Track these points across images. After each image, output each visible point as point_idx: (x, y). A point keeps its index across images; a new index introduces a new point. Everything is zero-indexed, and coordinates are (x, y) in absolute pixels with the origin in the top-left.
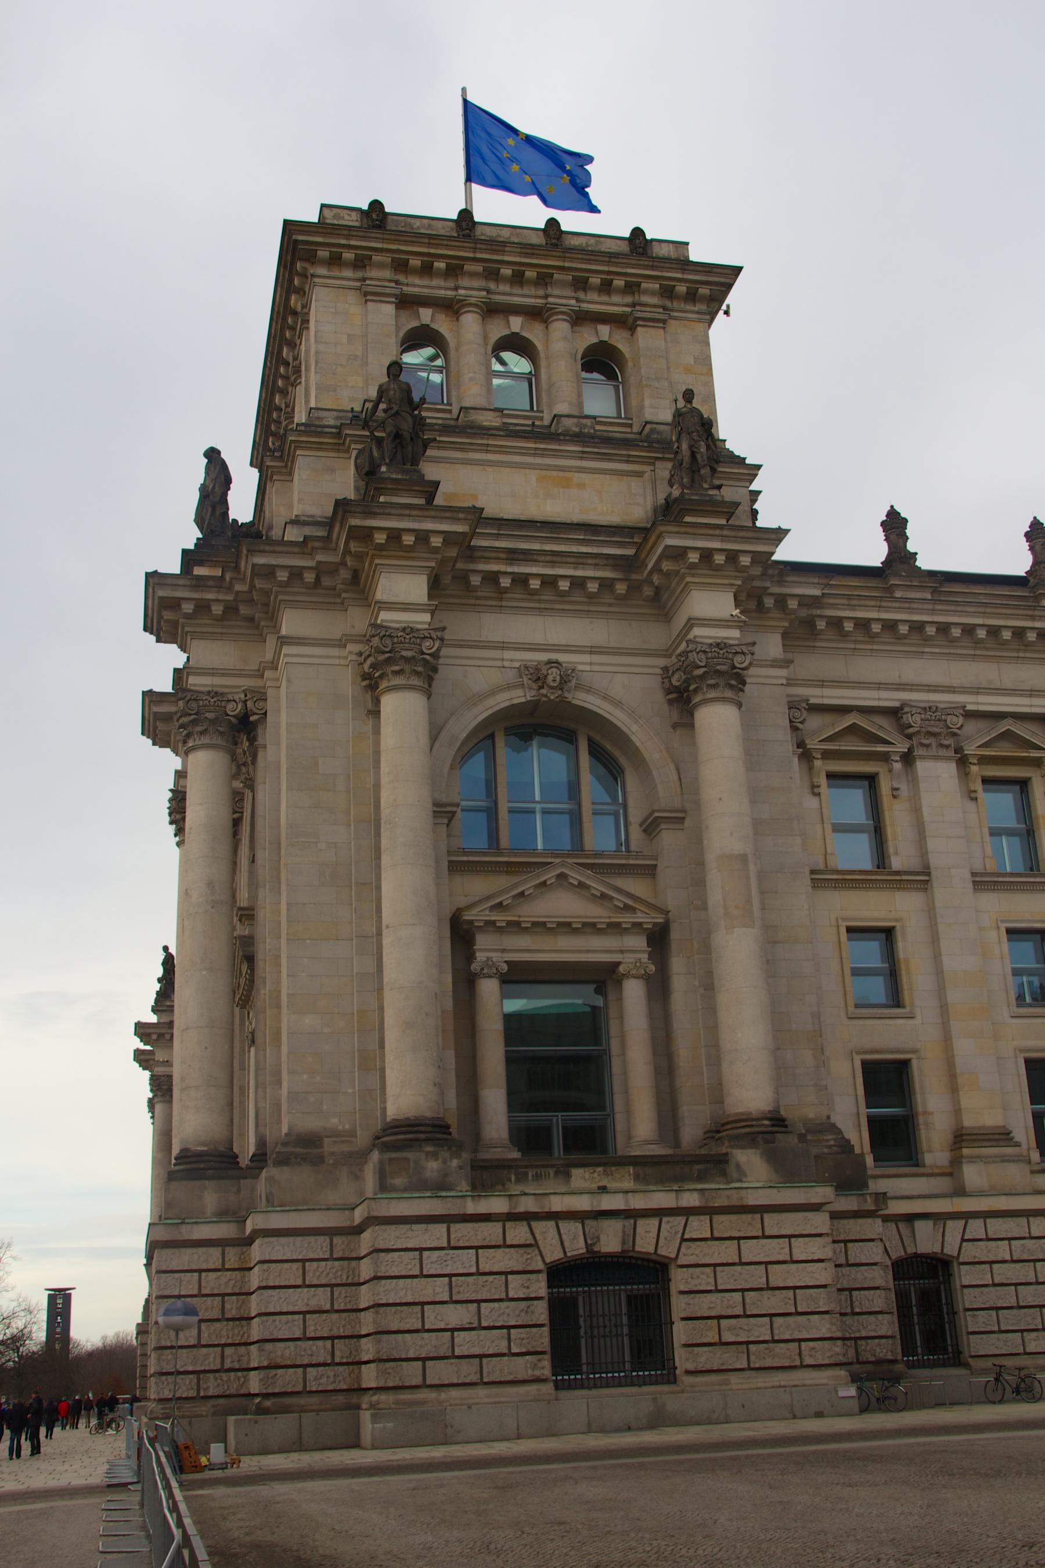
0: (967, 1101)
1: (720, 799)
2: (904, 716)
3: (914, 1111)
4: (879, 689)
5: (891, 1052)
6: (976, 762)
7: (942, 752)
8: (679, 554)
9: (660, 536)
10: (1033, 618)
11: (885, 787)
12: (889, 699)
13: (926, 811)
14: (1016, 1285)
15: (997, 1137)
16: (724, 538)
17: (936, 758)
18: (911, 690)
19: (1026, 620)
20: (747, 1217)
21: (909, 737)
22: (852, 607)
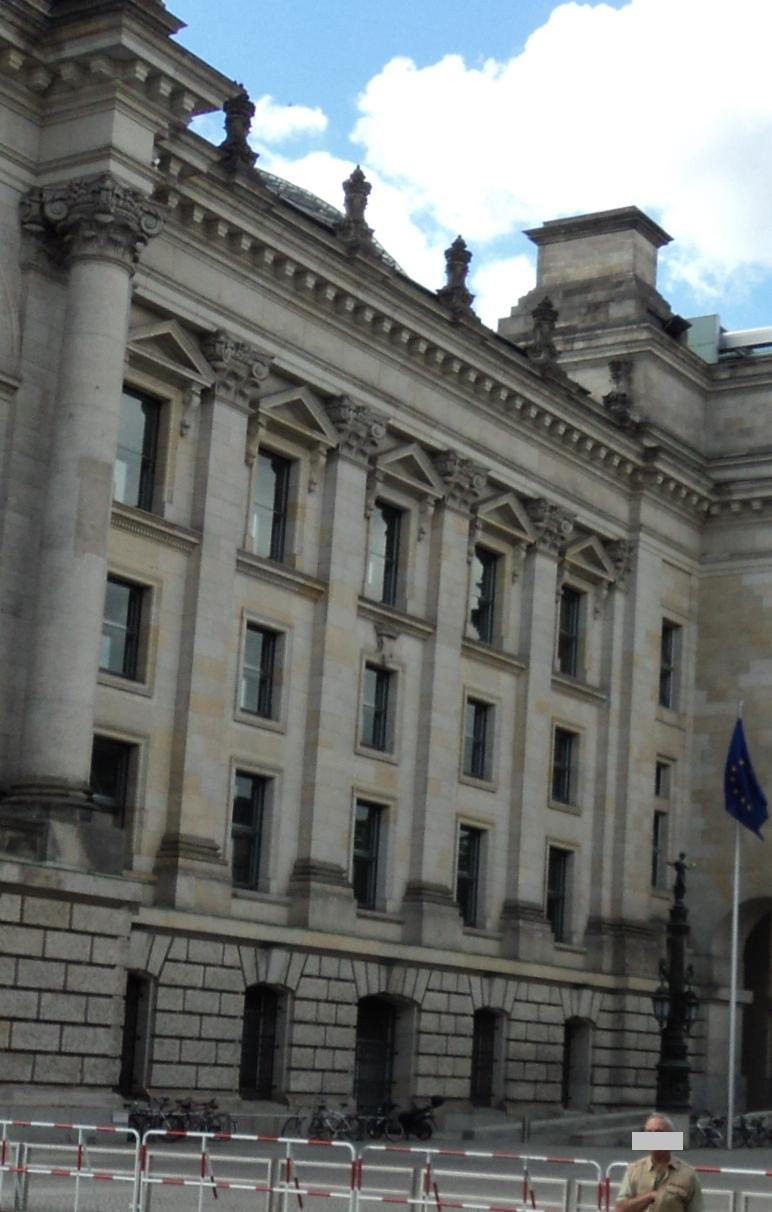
0: (190, 805)
1: (97, 388)
2: (218, 345)
3: (128, 804)
4: (199, 302)
5: (125, 732)
6: (265, 424)
7: (240, 401)
8: (129, 60)
9: (117, 28)
10: (359, 285)
11: (175, 416)
12: (207, 319)
13: (212, 463)
14: (201, 1015)
15: (206, 850)
16: (180, 67)
17: (233, 405)
18: (228, 317)
19: (352, 285)
20: (57, 904)
21: (215, 370)
22: (210, 195)
